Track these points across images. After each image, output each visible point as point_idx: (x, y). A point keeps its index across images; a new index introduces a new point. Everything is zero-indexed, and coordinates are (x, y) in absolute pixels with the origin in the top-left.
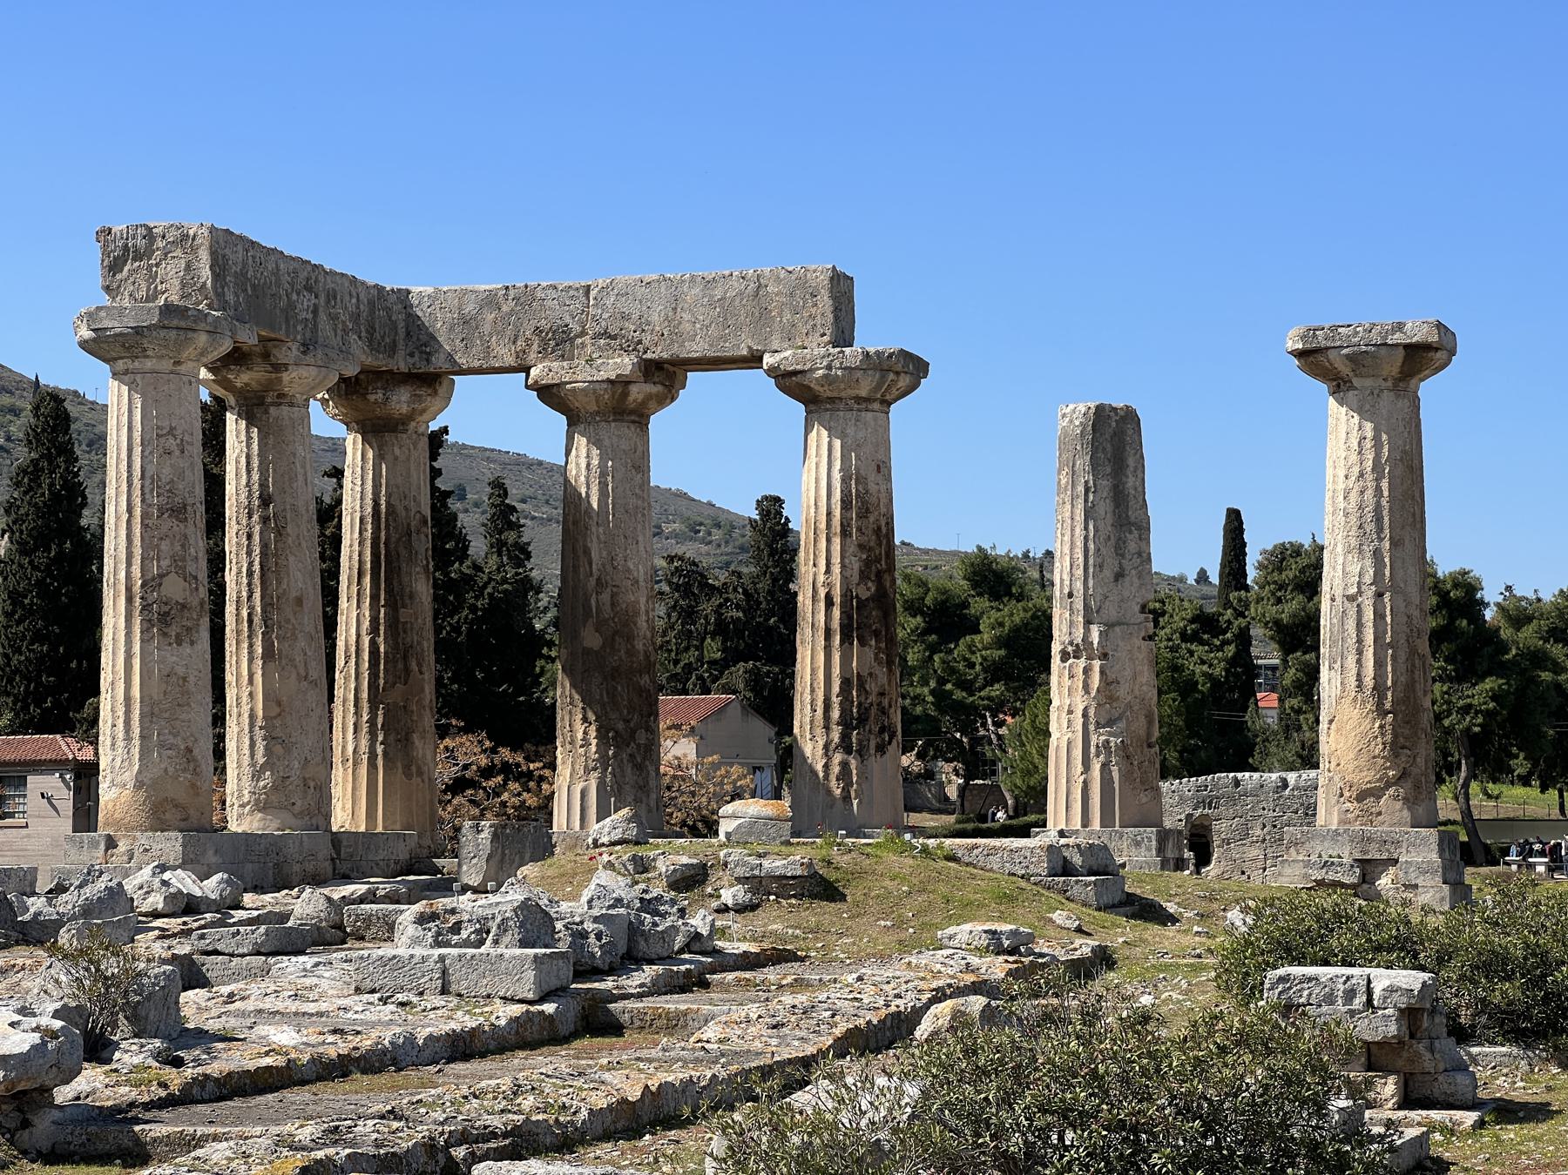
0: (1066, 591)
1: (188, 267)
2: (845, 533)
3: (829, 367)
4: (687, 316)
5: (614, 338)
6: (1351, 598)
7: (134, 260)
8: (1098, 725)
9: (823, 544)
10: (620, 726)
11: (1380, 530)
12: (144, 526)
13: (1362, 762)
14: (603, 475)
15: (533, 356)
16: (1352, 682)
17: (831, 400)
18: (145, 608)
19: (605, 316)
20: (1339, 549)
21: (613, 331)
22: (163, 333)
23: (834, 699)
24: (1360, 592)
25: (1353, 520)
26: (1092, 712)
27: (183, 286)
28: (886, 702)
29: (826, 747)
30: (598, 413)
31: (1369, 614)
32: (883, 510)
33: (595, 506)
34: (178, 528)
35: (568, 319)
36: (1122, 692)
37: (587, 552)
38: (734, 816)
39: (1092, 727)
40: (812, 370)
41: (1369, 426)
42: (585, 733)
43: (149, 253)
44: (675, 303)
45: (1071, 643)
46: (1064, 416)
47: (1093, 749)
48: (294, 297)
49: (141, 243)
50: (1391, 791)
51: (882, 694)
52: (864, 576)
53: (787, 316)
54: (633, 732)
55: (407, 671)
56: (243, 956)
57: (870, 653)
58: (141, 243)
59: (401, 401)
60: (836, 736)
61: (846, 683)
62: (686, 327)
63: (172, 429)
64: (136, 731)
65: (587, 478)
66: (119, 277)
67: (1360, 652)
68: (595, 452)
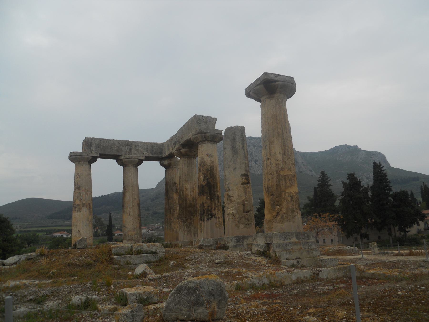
2: (200, 171)
10: (184, 219)
28: (210, 208)
32: (208, 164)
34: (78, 191)
36: (235, 198)
48: (122, 147)
51: (208, 206)
52: (203, 180)
54: (187, 220)
55: (171, 212)
57: (205, 197)
59: (166, 162)
61: (201, 205)
63: (78, 174)
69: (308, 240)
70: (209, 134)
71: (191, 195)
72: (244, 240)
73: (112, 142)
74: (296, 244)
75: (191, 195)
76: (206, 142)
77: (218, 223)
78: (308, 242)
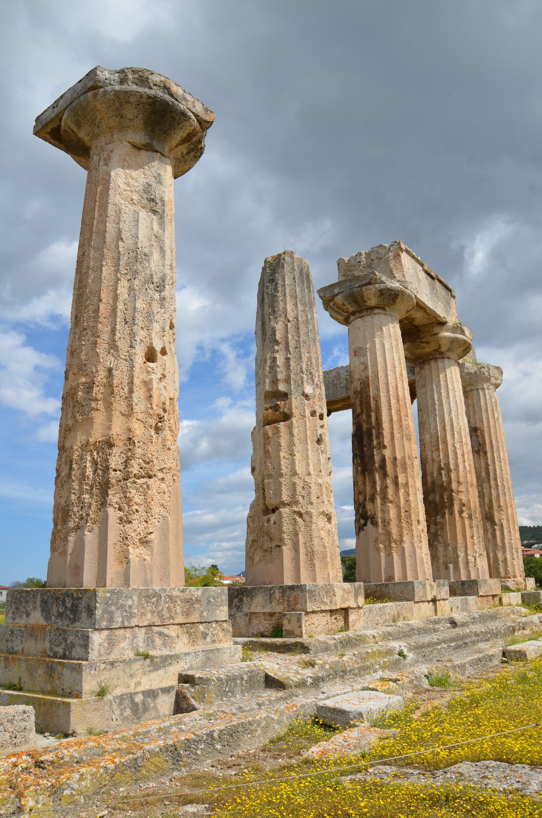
69: (73, 621)
70: (339, 297)
71: (433, 460)
72: (241, 600)
73: (334, 373)
74: (33, 632)
75: (433, 460)
76: (352, 317)
77: (383, 538)
78: (64, 631)
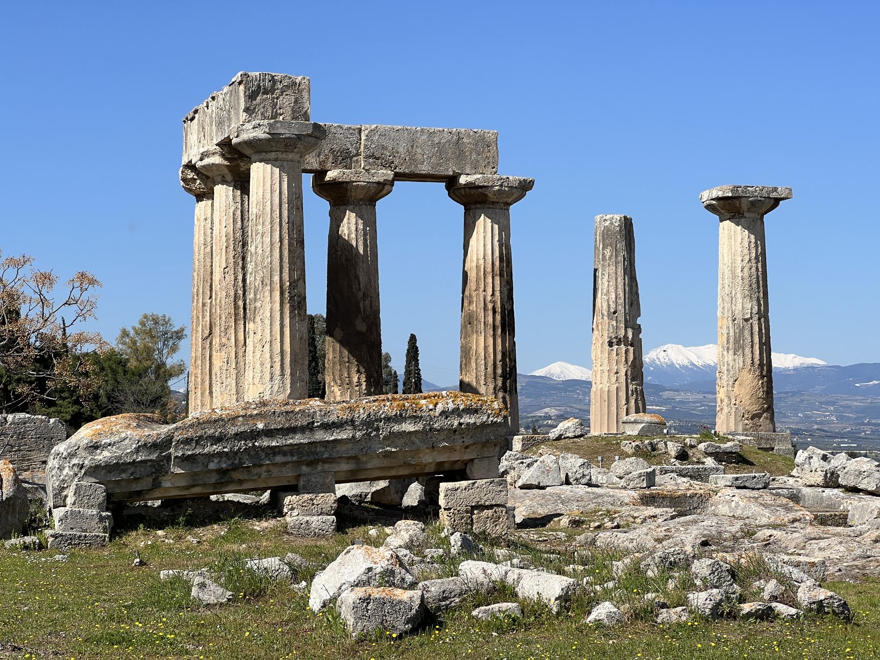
0: (612, 310)
1: (296, 102)
2: (501, 275)
3: (501, 186)
4: (419, 151)
5: (378, 159)
6: (746, 320)
7: (264, 93)
8: (632, 380)
9: (490, 280)
11: (758, 288)
12: (290, 250)
13: (753, 400)
14: (365, 235)
15: (329, 164)
16: (749, 361)
17: (493, 203)
18: (292, 298)
19: (373, 146)
20: (739, 295)
21: (377, 155)
22: (310, 139)
23: (498, 363)
24: (751, 318)
25: (747, 282)
26: (629, 373)
27: (293, 112)
29: (495, 388)
30: (361, 200)
31: (756, 328)
33: (361, 252)
35: (349, 146)
37: (357, 277)
38: (635, 422)
39: (629, 381)
40: (492, 186)
41: (752, 237)
42: (359, 378)
43: (272, 90)
44: (413, 142)
45: (616, 338)
46: (605, 220)
47: (630, 392)
49: (268, 84)
50: (765, 415)
53: (474, 156)
56: (759, 489)
58: (268, 84)
60: (500, 383)
62: (420, 157)
64: (288, 371)
65: (356, 235)
66: (254, 102)
67: (752, 347)
68: (360, 222)
